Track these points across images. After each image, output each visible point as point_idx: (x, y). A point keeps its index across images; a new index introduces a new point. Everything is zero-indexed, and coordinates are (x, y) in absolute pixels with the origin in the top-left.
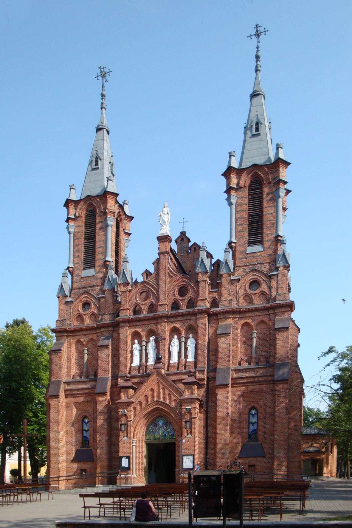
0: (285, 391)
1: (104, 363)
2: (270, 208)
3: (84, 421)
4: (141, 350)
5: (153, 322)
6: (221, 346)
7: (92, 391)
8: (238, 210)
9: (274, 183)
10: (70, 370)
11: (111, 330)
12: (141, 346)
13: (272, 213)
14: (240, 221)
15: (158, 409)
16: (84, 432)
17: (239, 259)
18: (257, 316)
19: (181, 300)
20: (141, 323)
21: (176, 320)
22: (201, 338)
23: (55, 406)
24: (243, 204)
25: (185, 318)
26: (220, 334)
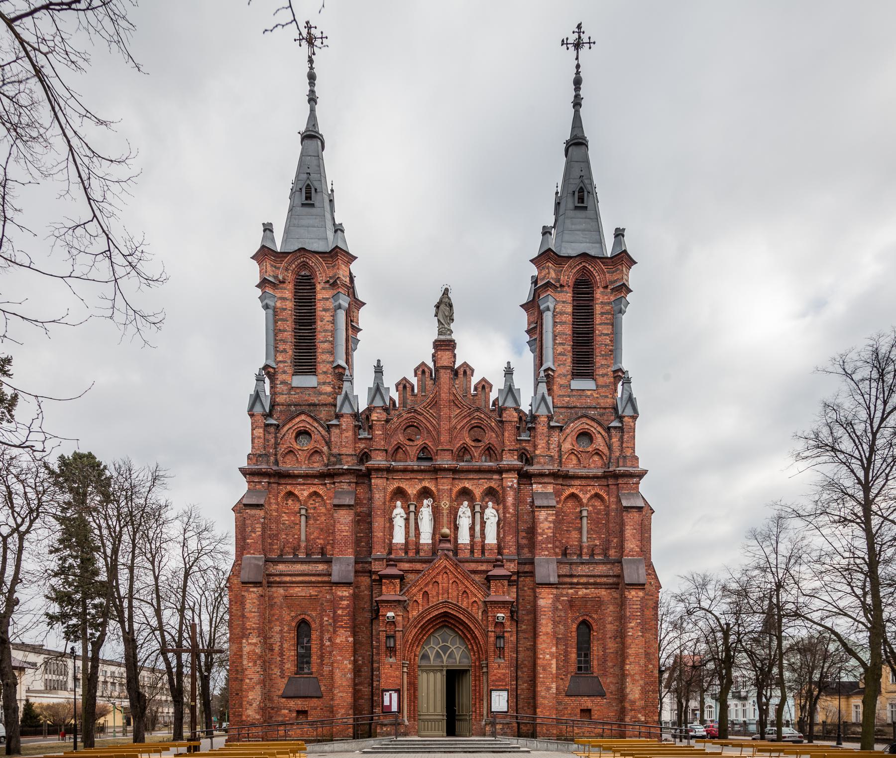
2: (606, 327)
4: (407, 520)
5: (427, 477)
8: (557, 321)
9: (612, 289)
12: (408, 514)
13: (607, 335)
14: (560, 338)
15: (445, 614)
17: (560, 396)
24: (565, 313)
26: (540, 507)
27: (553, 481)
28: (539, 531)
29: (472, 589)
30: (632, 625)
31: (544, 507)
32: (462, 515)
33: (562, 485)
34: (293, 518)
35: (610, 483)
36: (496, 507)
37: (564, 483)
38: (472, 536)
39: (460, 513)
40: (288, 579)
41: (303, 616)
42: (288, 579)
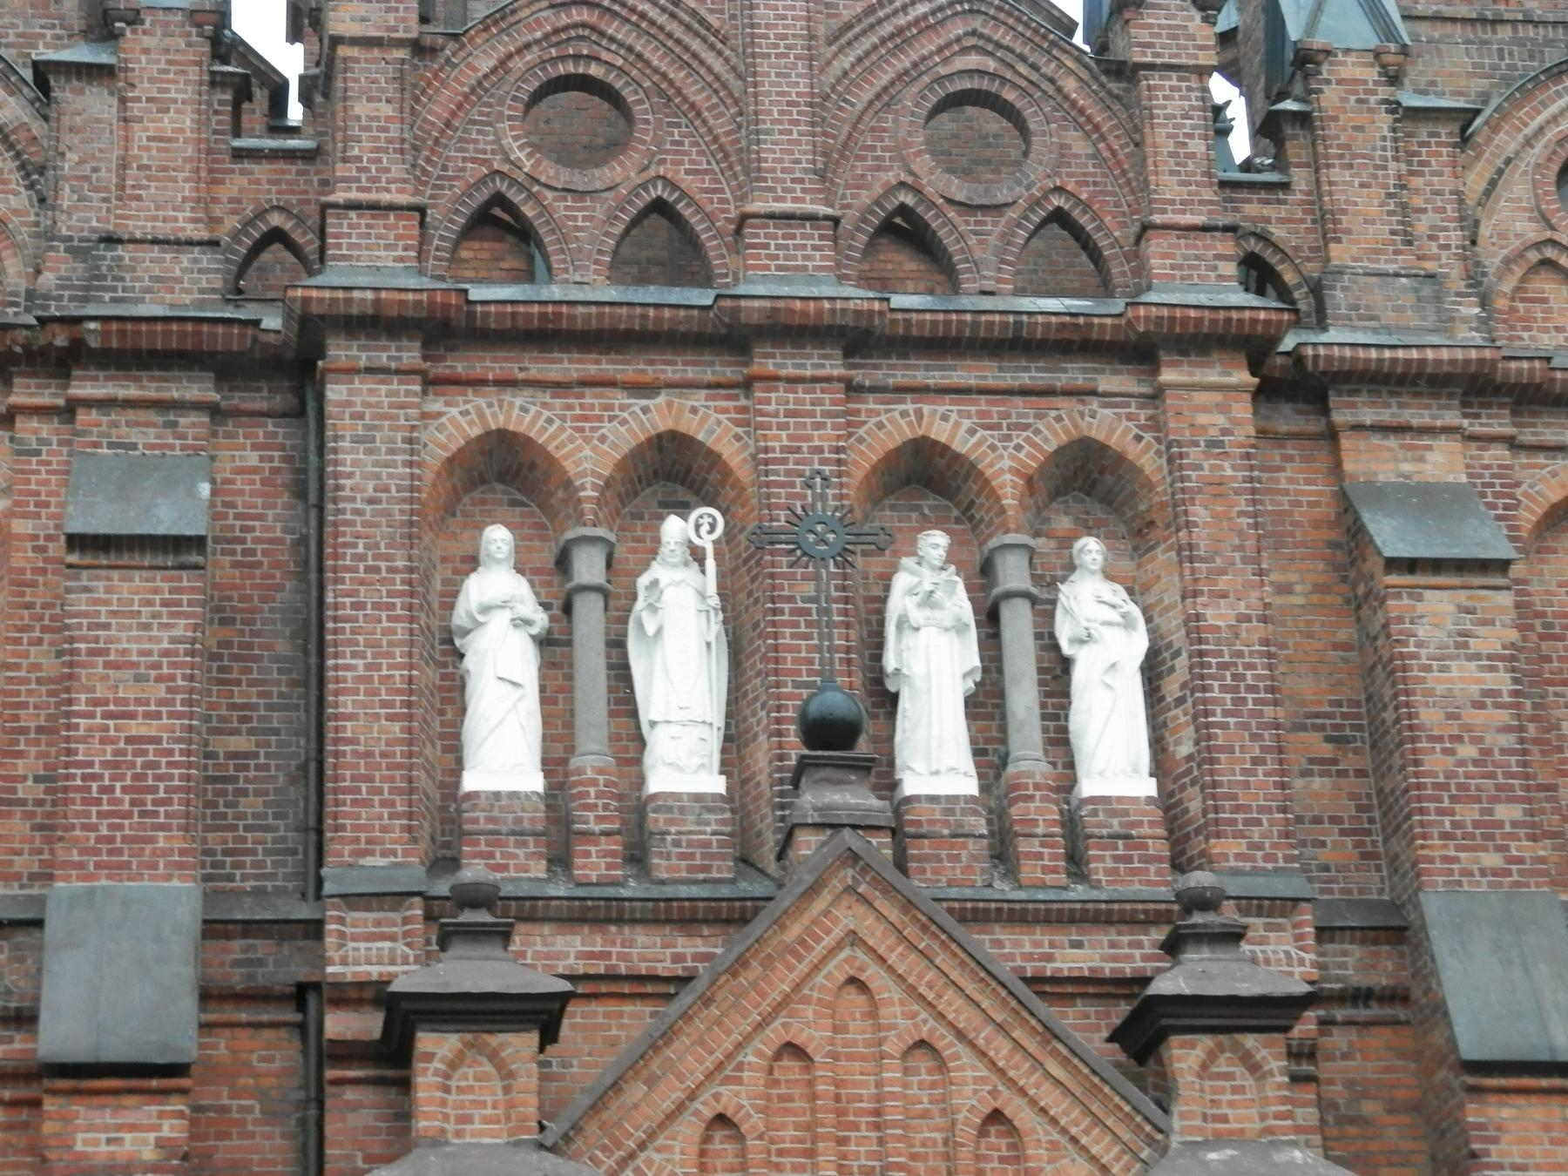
1: (136, 727)
5: (691, 373)
6: (1436, 681)
11: (197, 406)
19: (966, 208)
20: (566, 366)
21: (935, 378)
22: (1223, 582)
25: (1032, 374)
26: (1411, 565)
28: (1429, 716)
29: (1048, 1096)
31: (1437, 565)
32: (916, 615)
33: (1511, 443)
36: (1126, 566)
37: (1527, 436)
39: (900, 602)
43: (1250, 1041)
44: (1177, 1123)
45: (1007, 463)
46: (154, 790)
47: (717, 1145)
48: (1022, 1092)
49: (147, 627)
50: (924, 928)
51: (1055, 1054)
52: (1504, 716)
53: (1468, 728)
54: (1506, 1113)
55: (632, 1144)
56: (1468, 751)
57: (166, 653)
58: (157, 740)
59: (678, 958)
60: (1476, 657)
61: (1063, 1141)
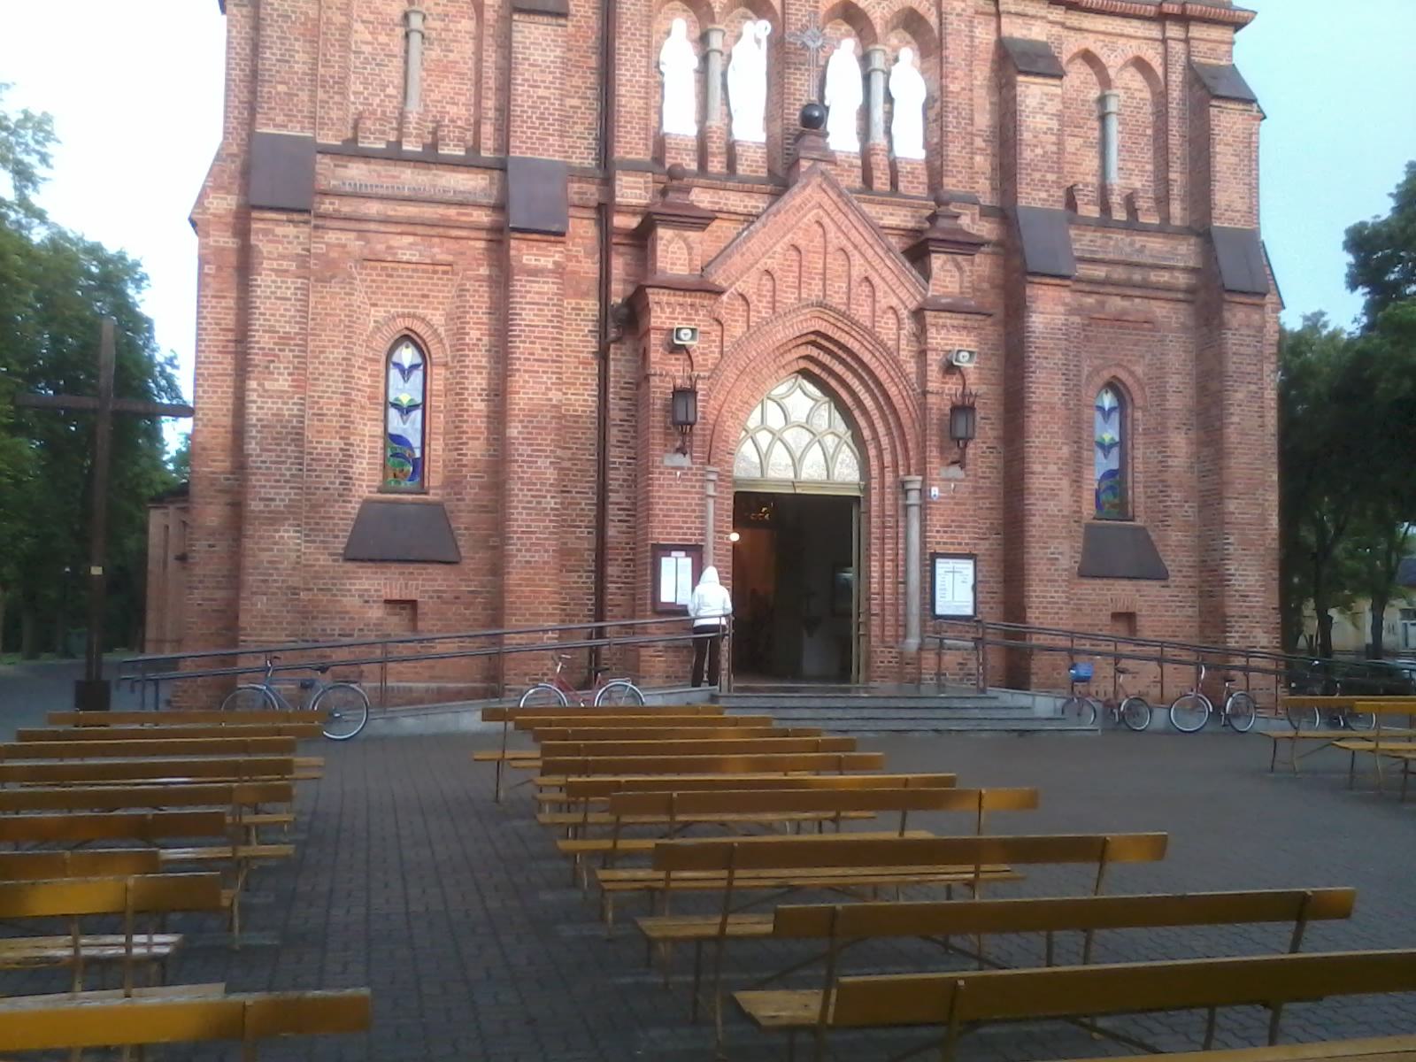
0: (1254, 336)
1: (541, 92)
3: (395, 358)
7: (464, 218)
10: (337, 98)
16: (393, 412)
18: (1122, 35)
23: (285, 264)
27: (1043, 12)
28: (1026, 136)
29: (886, 273)
30: (1240, 396)
33: (1063, 25)
34: (383, 39)
35: (1169, 34)
37: (1068, 23)
38: (865, 132)
40: (373, 208)
41: (408, 323)
42: (373, 208)
43: (960, 258)
44: (931, 287)
45: (878, 14)
46: (548, 119)
47: (764, 282)
48: (876, 271)
49: (544, 50)
50: (846, 204)
51: (890, 258)
52: (1054, 139)
53: (1041, 142)
54: (1040, 292)
55: (734, 279)
56: (1039, 151)
57: (552, 62)
58: (549, 99)
59: (745, 207)
60: (1046, 114)
61: (889, 290)
